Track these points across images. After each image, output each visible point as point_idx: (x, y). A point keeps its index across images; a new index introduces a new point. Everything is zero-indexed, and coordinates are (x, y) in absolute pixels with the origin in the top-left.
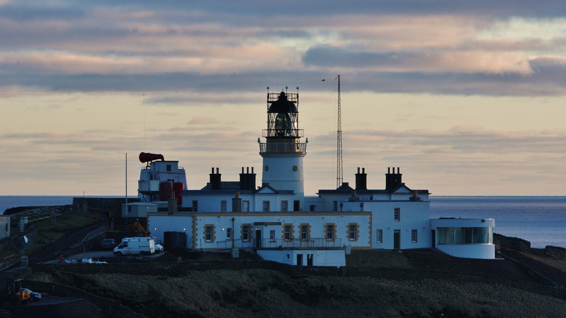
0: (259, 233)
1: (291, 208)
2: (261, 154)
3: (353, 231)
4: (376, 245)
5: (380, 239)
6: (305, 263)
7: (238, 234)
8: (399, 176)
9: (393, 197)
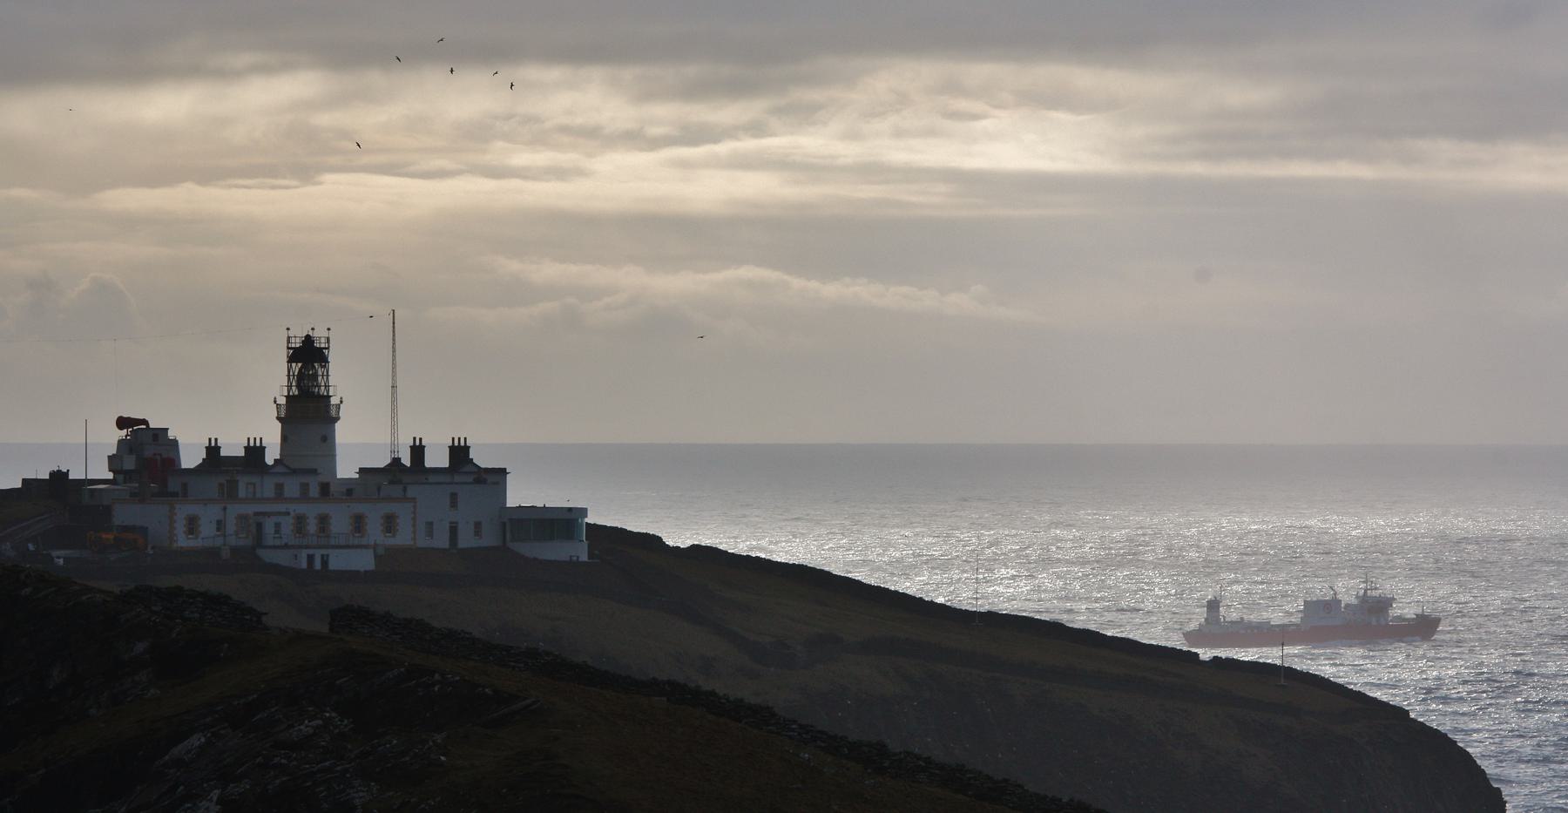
0: (259, 526)
1: (314, 491)
2: (278, 418)
3: (390, 524)
4: (423, 542)
5: (430, 533)
6: (318, 565)
7: (231, 527)
8: (466, 449)
9: (457, 478)
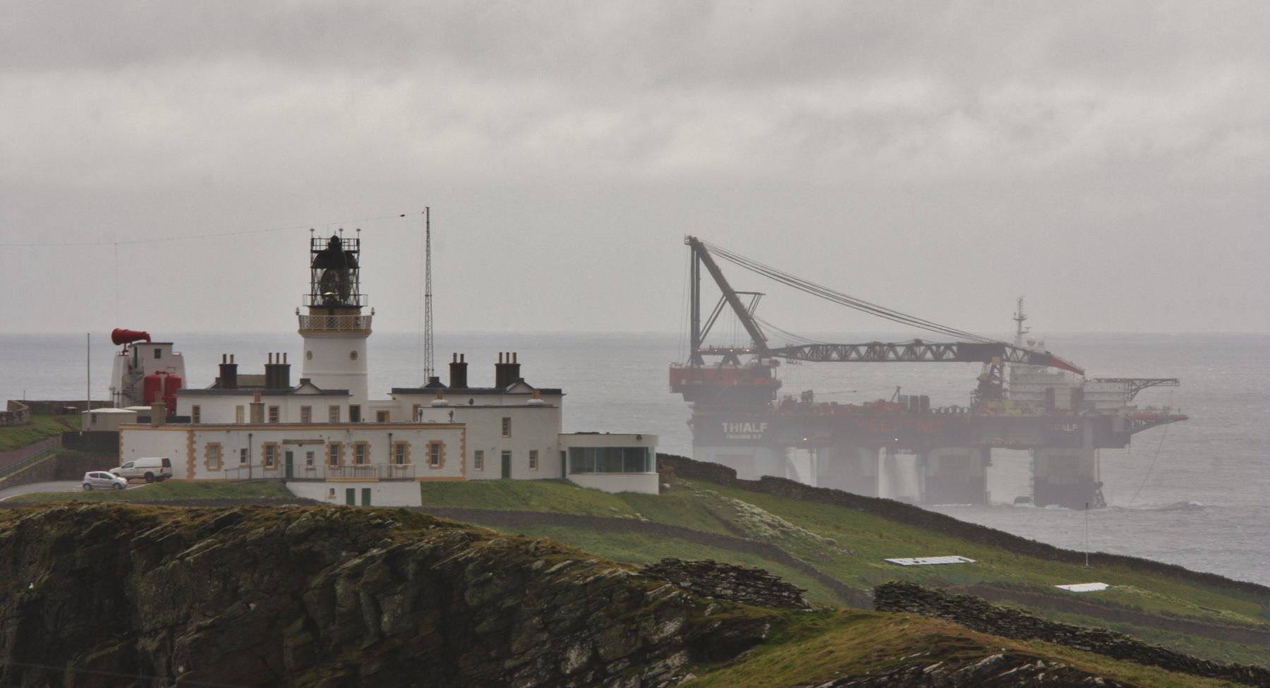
0: (289, 455)
1: (345, 417)
3: (435, 454)
4: (473, 474)
6: (358, 502)
7: (257, 457)
8: (515, 368)
9: (506, 401)
